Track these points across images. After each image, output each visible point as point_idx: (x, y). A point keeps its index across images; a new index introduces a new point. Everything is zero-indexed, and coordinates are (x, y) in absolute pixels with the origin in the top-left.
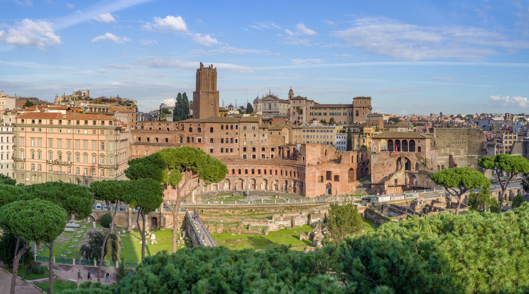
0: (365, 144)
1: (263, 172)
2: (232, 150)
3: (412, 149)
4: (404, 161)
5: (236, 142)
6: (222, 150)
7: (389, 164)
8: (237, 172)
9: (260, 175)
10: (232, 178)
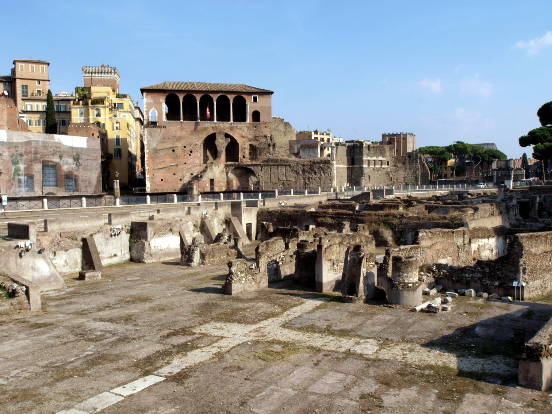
0: (101, 120)
3: (240, 116)
4: (221, 143)
7: (188, 149)
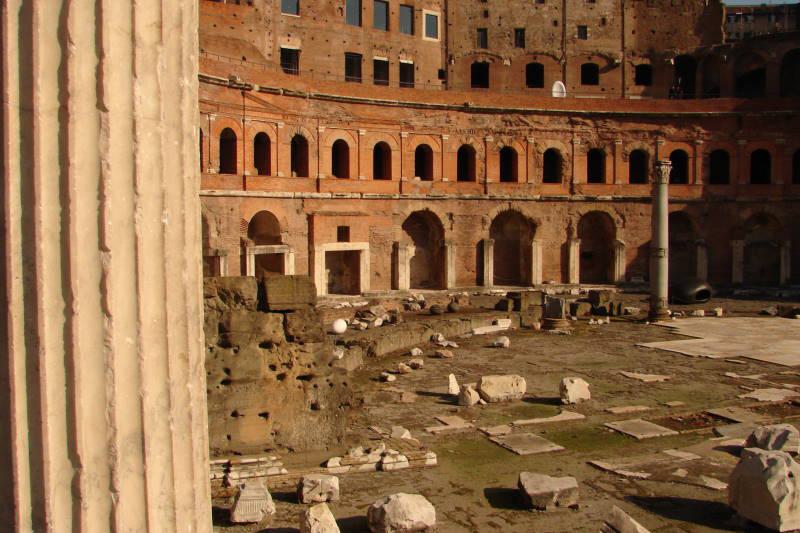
2: (407, 72)
5: (432, 32)
6: (353, 63)
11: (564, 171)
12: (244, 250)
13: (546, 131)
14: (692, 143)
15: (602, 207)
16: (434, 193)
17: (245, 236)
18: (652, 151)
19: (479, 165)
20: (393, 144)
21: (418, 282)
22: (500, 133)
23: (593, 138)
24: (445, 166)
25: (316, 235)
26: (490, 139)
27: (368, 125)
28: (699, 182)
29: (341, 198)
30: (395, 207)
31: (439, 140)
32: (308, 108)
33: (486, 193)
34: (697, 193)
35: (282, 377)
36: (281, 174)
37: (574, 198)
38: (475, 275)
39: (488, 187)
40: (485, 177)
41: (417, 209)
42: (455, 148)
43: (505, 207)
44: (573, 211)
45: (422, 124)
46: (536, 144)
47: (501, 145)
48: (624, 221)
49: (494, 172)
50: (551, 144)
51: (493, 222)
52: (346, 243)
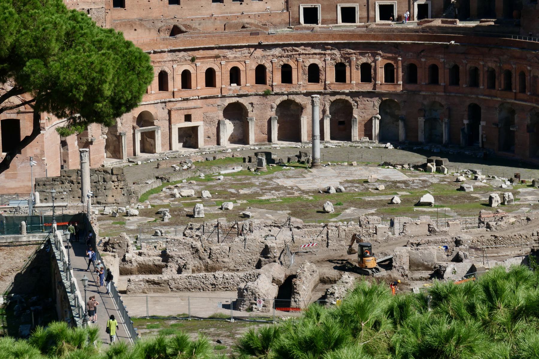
1: (381, 73)
8: (275, 77)
9: (368, 87)
10: (255, 100)
11: (320, 77)
12: (134, 131)
13: (309, 54)
14: (395, 60)
15: (344, 97)
16: (241, 93)
17: (135, 124)
18: (373, 64)
19: (268, 75)
20: (216, 68)
21: (236, 139)
22: (281, 57)
23: (338, 56)
24: (248, 77)
25: (172, 120)
26: (275, 60)
27: (202, 60)
28: (401, 82)
29: (187, 100)
30: (219, 101)
31: (244, 64)
32: (168, 57)
33: (273, 91)
34: (400, 89)
35: (116, 188)
36: (153, 92)
37: (326, 91)
38: (266, 136)
39: (274, 87)
40: (272, 82)
41: (231, 102)
42: (254, 67)
43: (285, 98)
44: (327, 99)
45: (234, 55)
46: (303, 62)
47: (282, 63)
48: (358, 105)
49: (278, 77)
50: (312, 61)
51: (278, 106)
52: (189, 123)
